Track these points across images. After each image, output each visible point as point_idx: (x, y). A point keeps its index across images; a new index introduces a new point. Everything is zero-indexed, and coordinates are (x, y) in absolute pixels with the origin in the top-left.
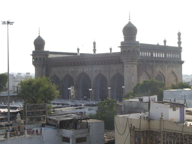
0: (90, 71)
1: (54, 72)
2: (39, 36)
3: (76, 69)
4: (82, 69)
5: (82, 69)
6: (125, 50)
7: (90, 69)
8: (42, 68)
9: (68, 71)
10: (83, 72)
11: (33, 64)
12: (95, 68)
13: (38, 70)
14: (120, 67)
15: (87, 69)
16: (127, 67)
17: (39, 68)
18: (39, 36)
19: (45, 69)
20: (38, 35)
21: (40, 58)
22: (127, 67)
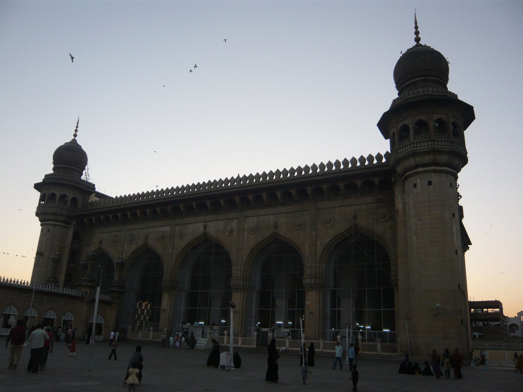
0: (231, 231)
1: (101, 243)
2: (74, 141)
3: (178, 228)
4: (202, 224)
5: (201, 226)
6: (423, 118)
7: (235, 223)
8: (65, 227)
9: (146, 238)
10: (205, 233)
11: (37, 214)
12: (254, 220)
13: (49, 230)
14: (364, 207)
15: (221, 223)
16: (430, 183)
17: (55, 225)
18: (74, 141)
19: (71, 233)
20: (73, 138)
21: (63, 197)
22: (430, 183)
